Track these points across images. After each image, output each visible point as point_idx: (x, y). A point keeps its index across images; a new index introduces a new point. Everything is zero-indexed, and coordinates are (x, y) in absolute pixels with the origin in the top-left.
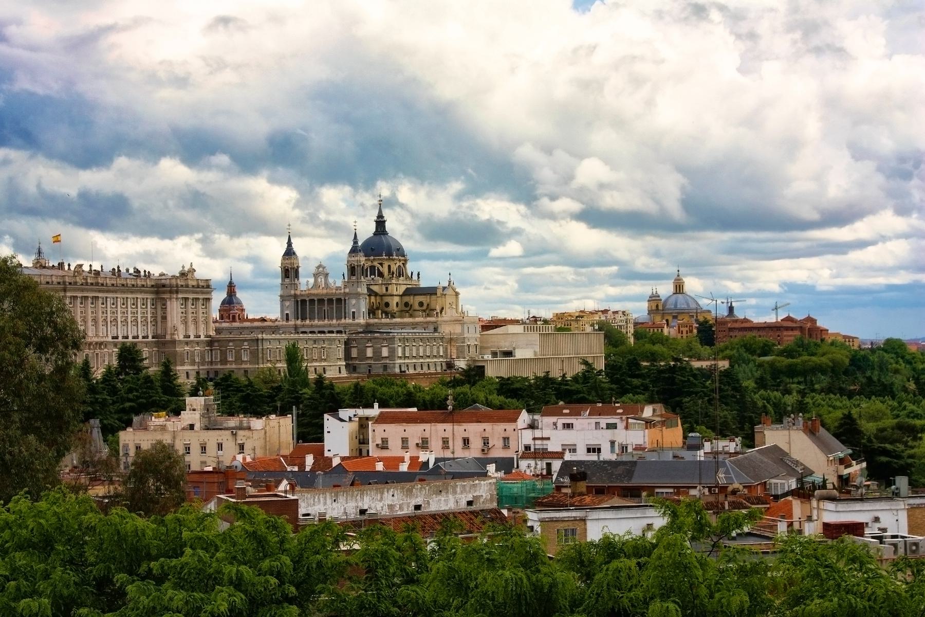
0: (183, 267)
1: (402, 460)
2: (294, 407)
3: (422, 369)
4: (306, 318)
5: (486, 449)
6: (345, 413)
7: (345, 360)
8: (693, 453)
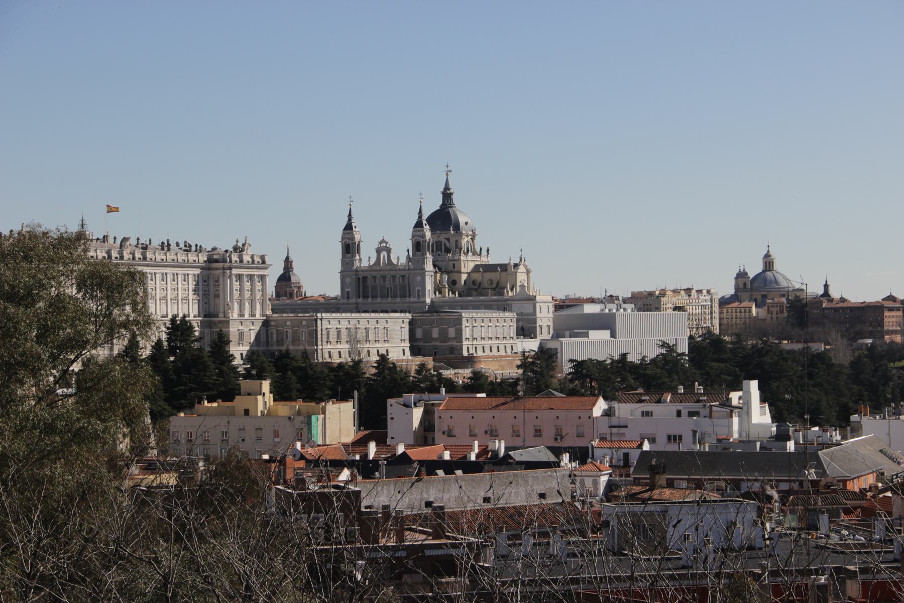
0: (237, 241)
3: (491, 351)
4: (368, 297)
5: (559, 438)
8: (782, 443)
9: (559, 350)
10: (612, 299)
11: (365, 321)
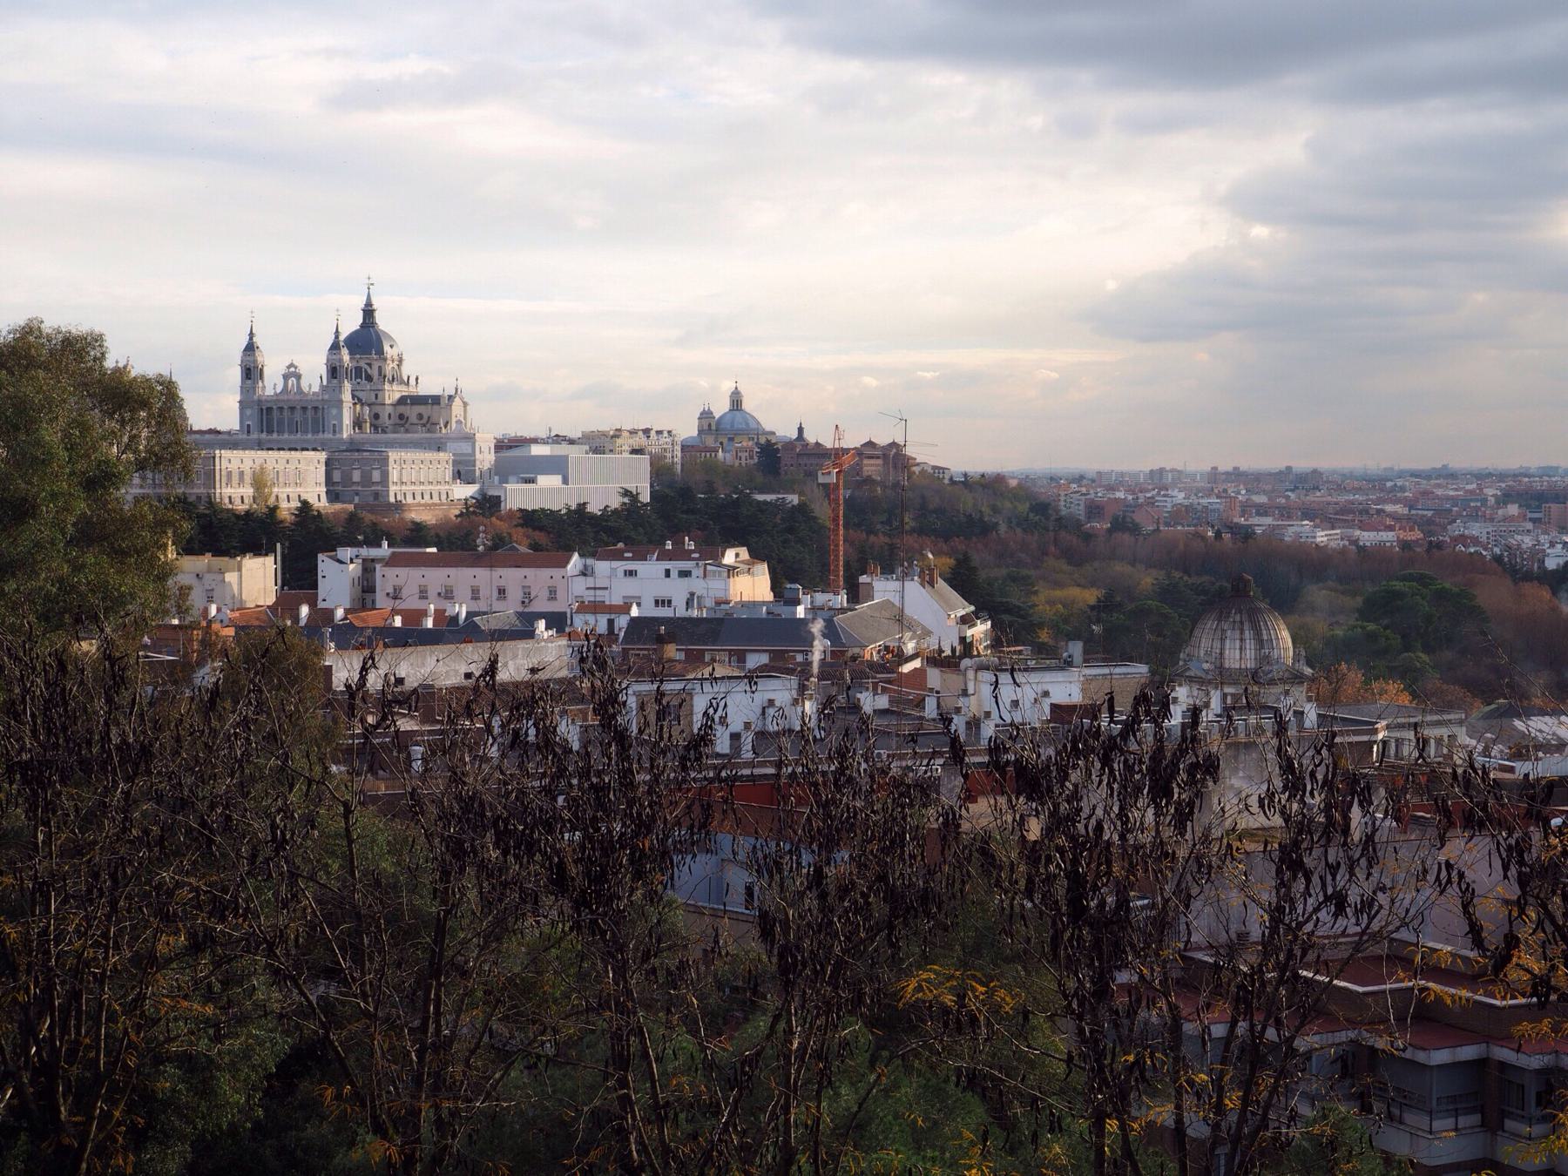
0: (117, 362)
1: (424, 613)
2: (278, 545)
5: (527, 600)
6: (346, 553)
7: (326, 485)
9: (502, 499)
10: (558, 439)
11: (274, 460)
